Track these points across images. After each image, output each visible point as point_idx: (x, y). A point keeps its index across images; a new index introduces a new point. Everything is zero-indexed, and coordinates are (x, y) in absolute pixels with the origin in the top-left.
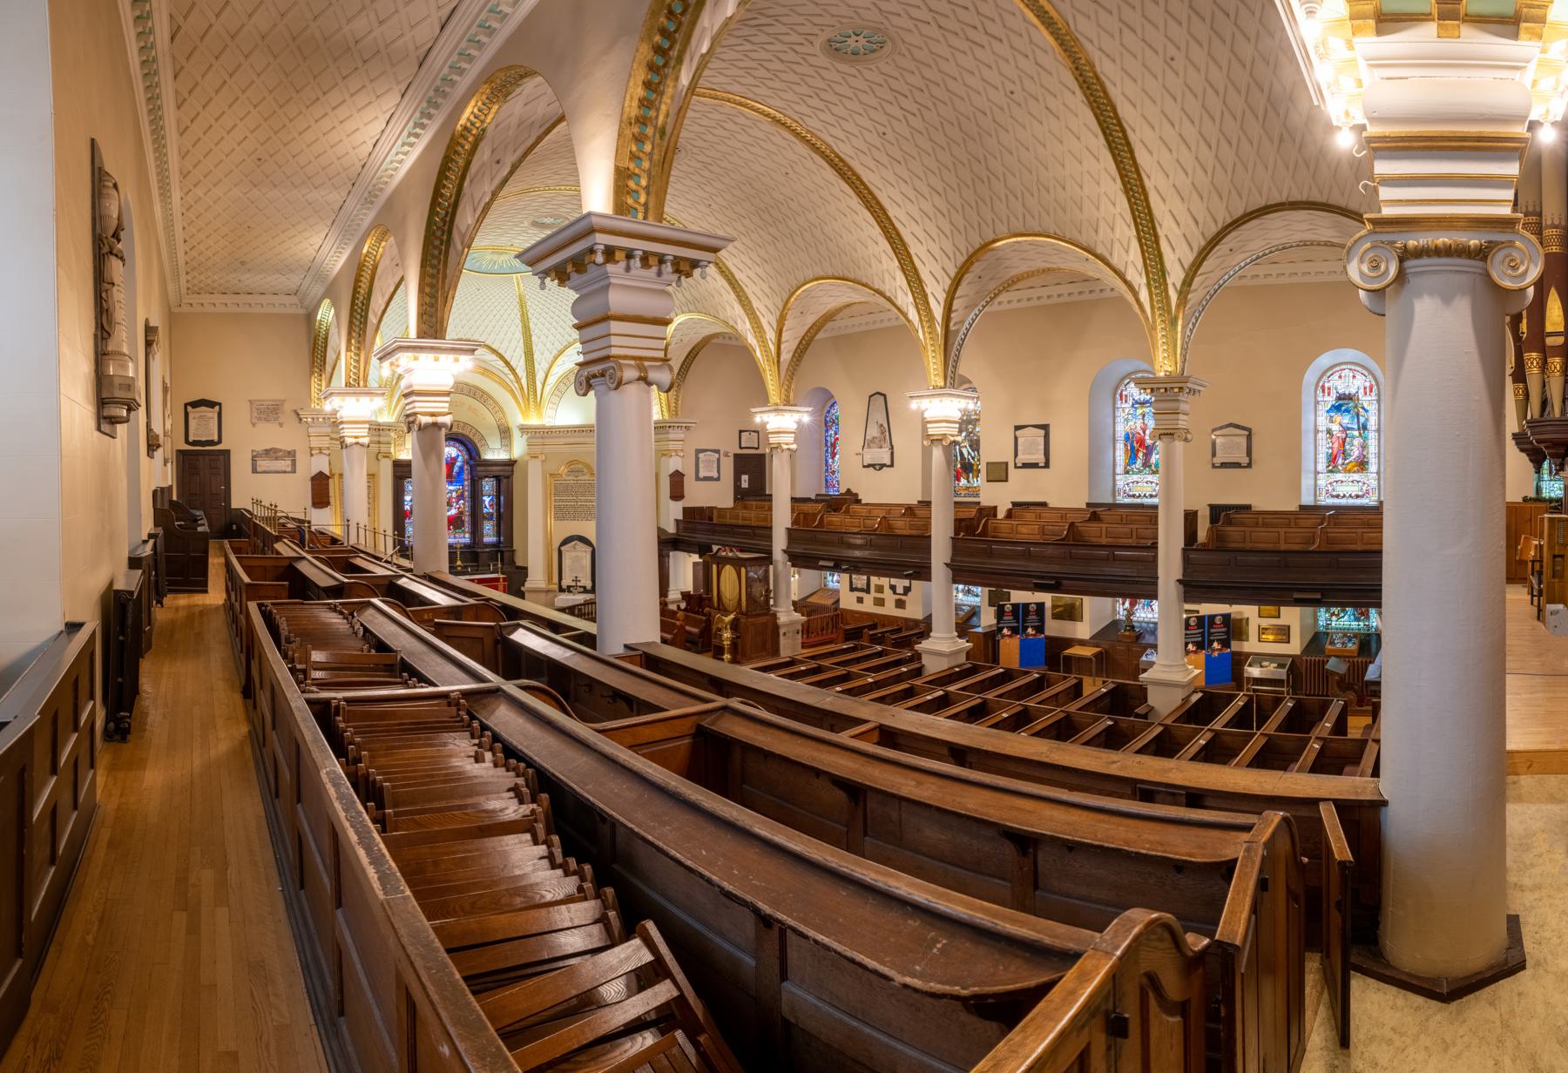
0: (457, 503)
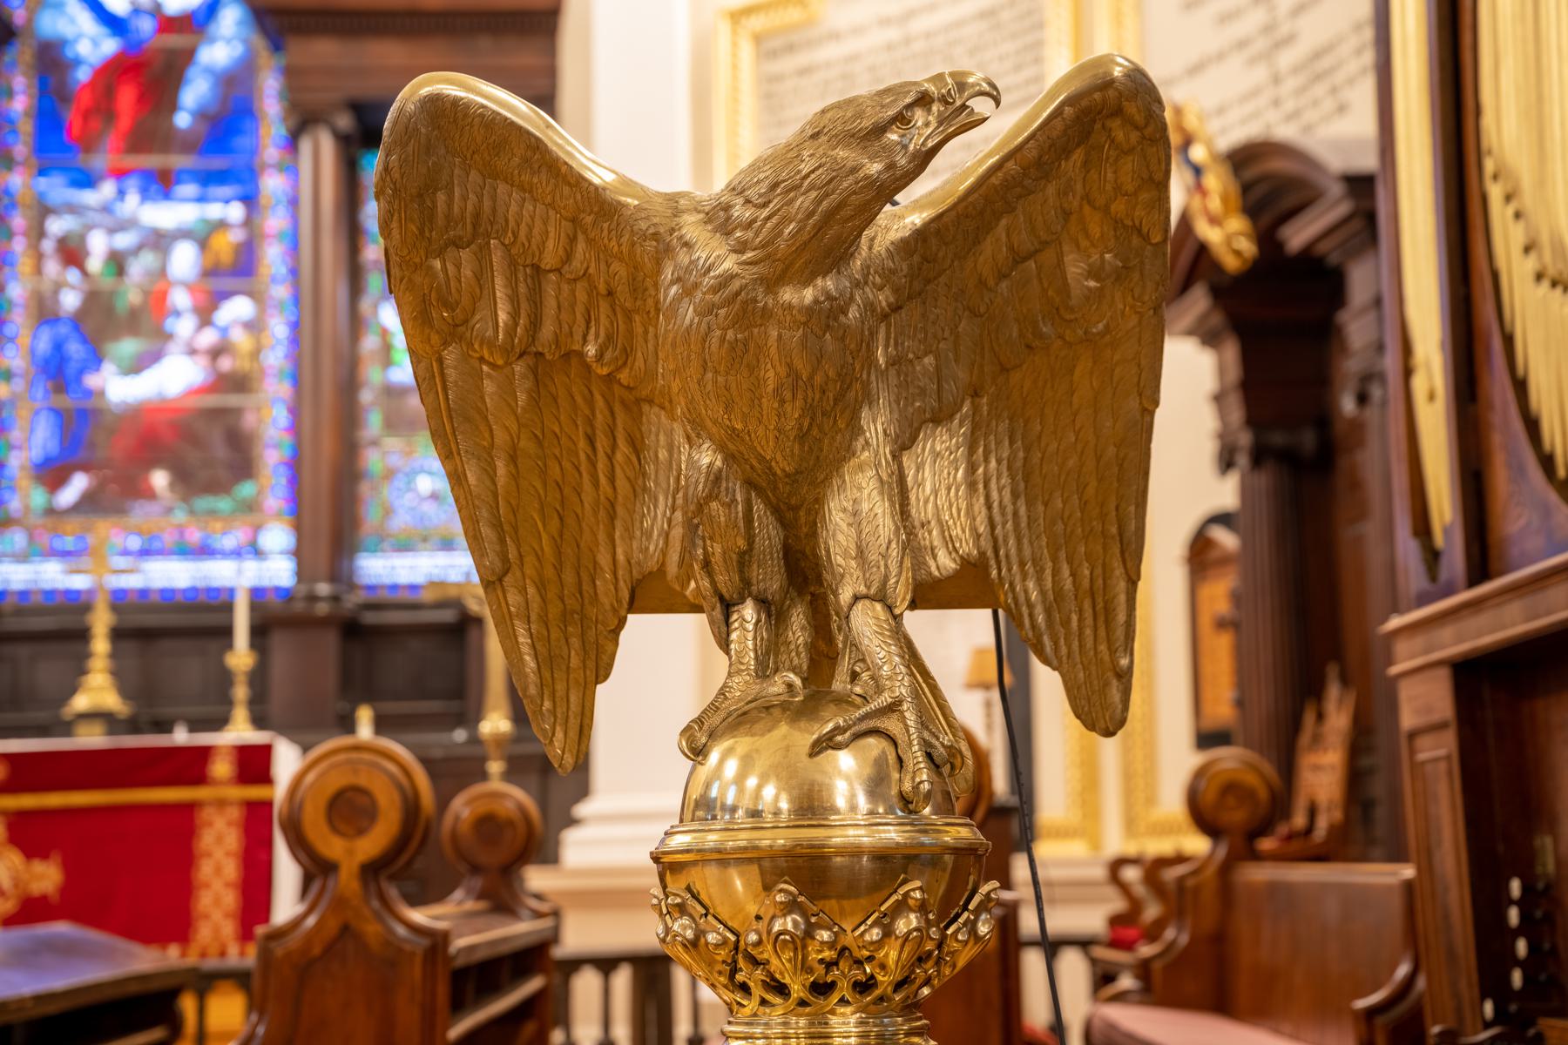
0: (205, 315)
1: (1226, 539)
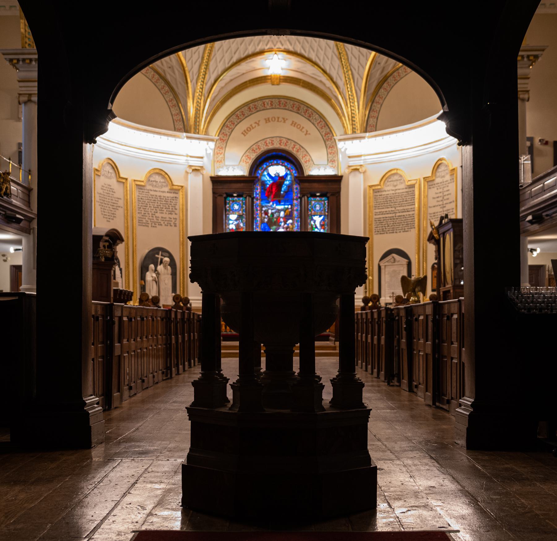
1: (436, 266)
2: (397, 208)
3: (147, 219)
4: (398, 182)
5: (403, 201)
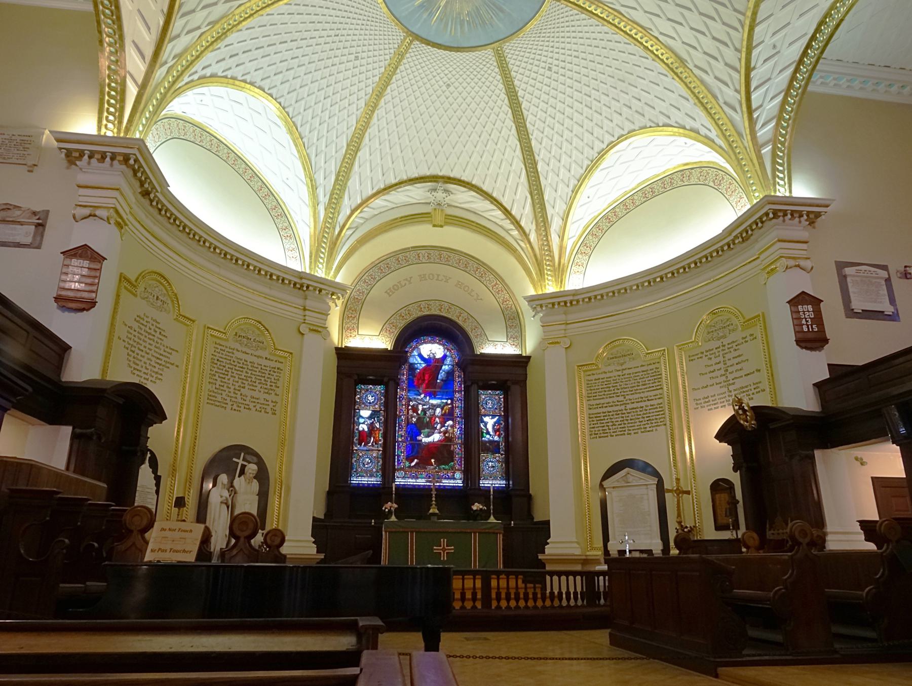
2: (627, 397)
3: (224, 396)
4: (627, 358)
5: (638, 386)
